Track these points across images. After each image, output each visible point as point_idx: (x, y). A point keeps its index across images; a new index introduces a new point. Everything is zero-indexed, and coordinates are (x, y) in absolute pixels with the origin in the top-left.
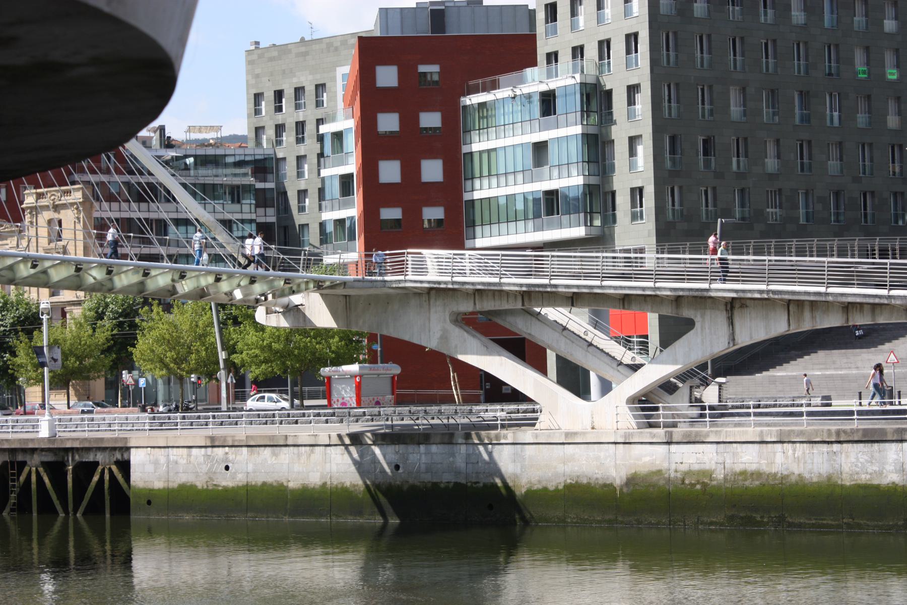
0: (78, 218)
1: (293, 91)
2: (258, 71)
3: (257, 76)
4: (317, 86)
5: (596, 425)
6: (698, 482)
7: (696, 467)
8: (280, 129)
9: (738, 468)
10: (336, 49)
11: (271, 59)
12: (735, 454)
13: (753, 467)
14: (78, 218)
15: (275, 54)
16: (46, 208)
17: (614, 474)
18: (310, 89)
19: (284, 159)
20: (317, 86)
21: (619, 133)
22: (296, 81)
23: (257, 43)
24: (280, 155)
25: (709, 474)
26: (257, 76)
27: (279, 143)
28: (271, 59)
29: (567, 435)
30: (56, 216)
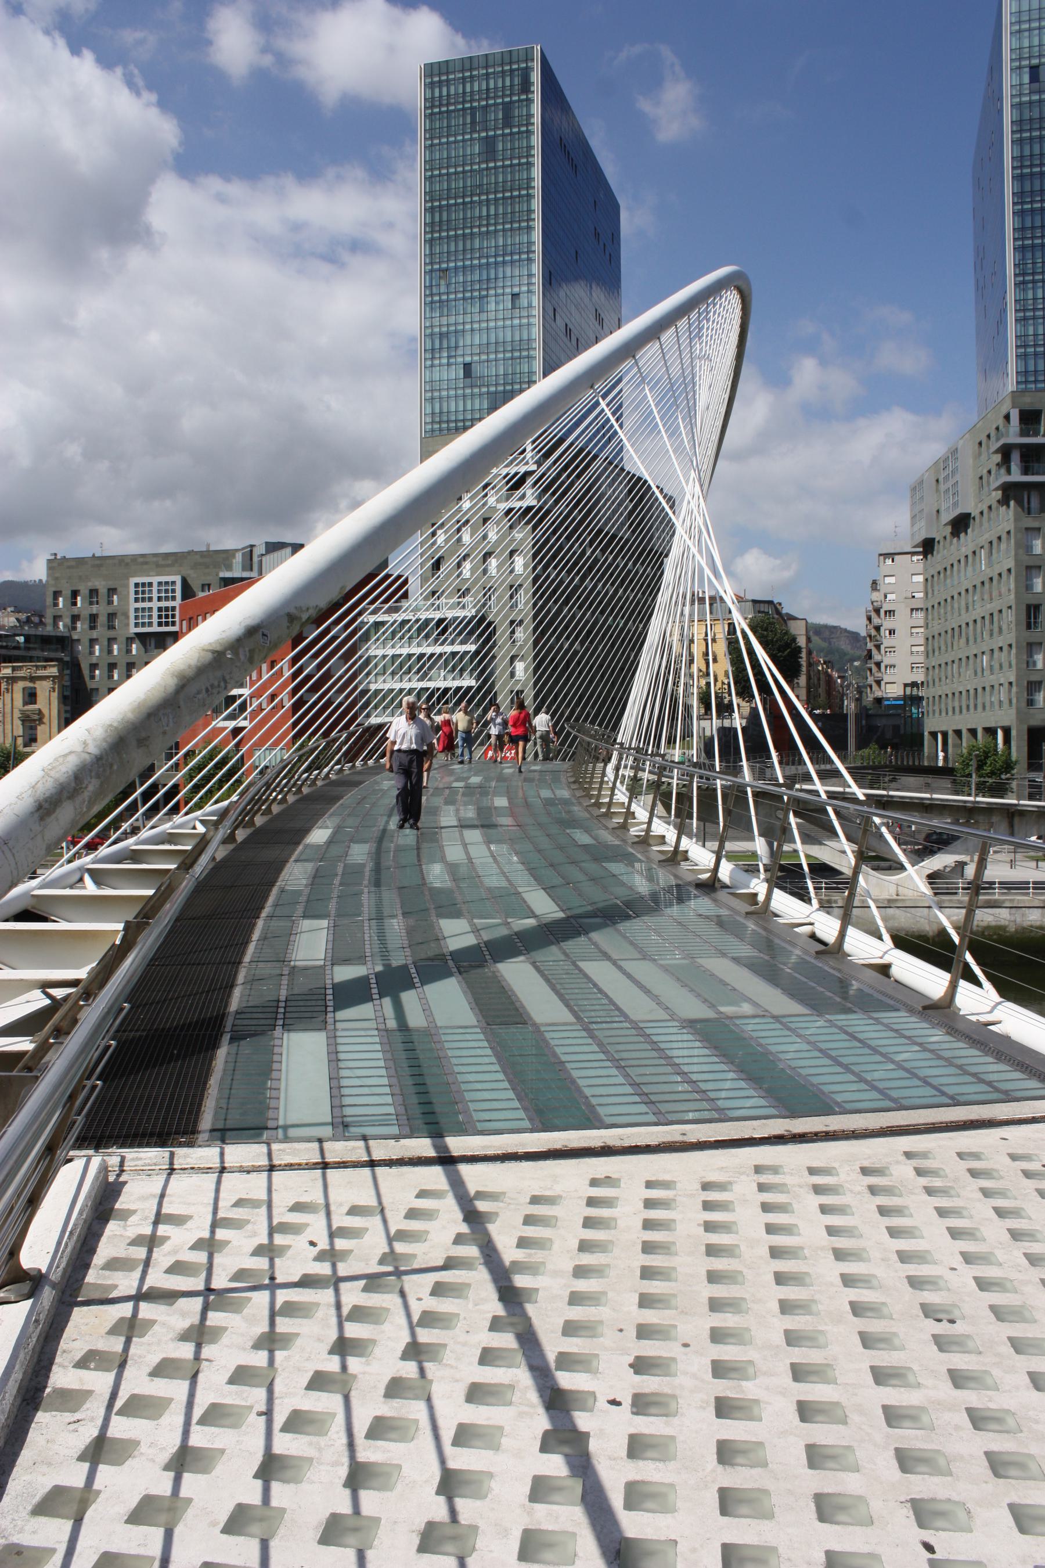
0: (54, 689)
1: (106, 591)
2: (57, 575)
3: (56, 579)
4: (109, 590)
5: (900, 892)
6: (995, 934)
7: (994, 924)
8: (75, 618)
9: (1026, 924)
10: (127, 564)
11: (69, 567)
12: (1023, 915)
13: (1038, 924)
14: (54, 689)
15: (73, 563)
16: (23, 679)
17: (927, 928)
18: (103, 591)
19: (78, 640)
20: (109, 590)
21: (502, 651)
22: (90, 585)
23: (55, 554)
24: (75, 637)
25: (1003, 928)
26: (56, 579)
27: (75, 628)
28: (69, 567)
29: (889, 901)
30: (31, 685)
